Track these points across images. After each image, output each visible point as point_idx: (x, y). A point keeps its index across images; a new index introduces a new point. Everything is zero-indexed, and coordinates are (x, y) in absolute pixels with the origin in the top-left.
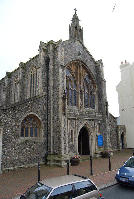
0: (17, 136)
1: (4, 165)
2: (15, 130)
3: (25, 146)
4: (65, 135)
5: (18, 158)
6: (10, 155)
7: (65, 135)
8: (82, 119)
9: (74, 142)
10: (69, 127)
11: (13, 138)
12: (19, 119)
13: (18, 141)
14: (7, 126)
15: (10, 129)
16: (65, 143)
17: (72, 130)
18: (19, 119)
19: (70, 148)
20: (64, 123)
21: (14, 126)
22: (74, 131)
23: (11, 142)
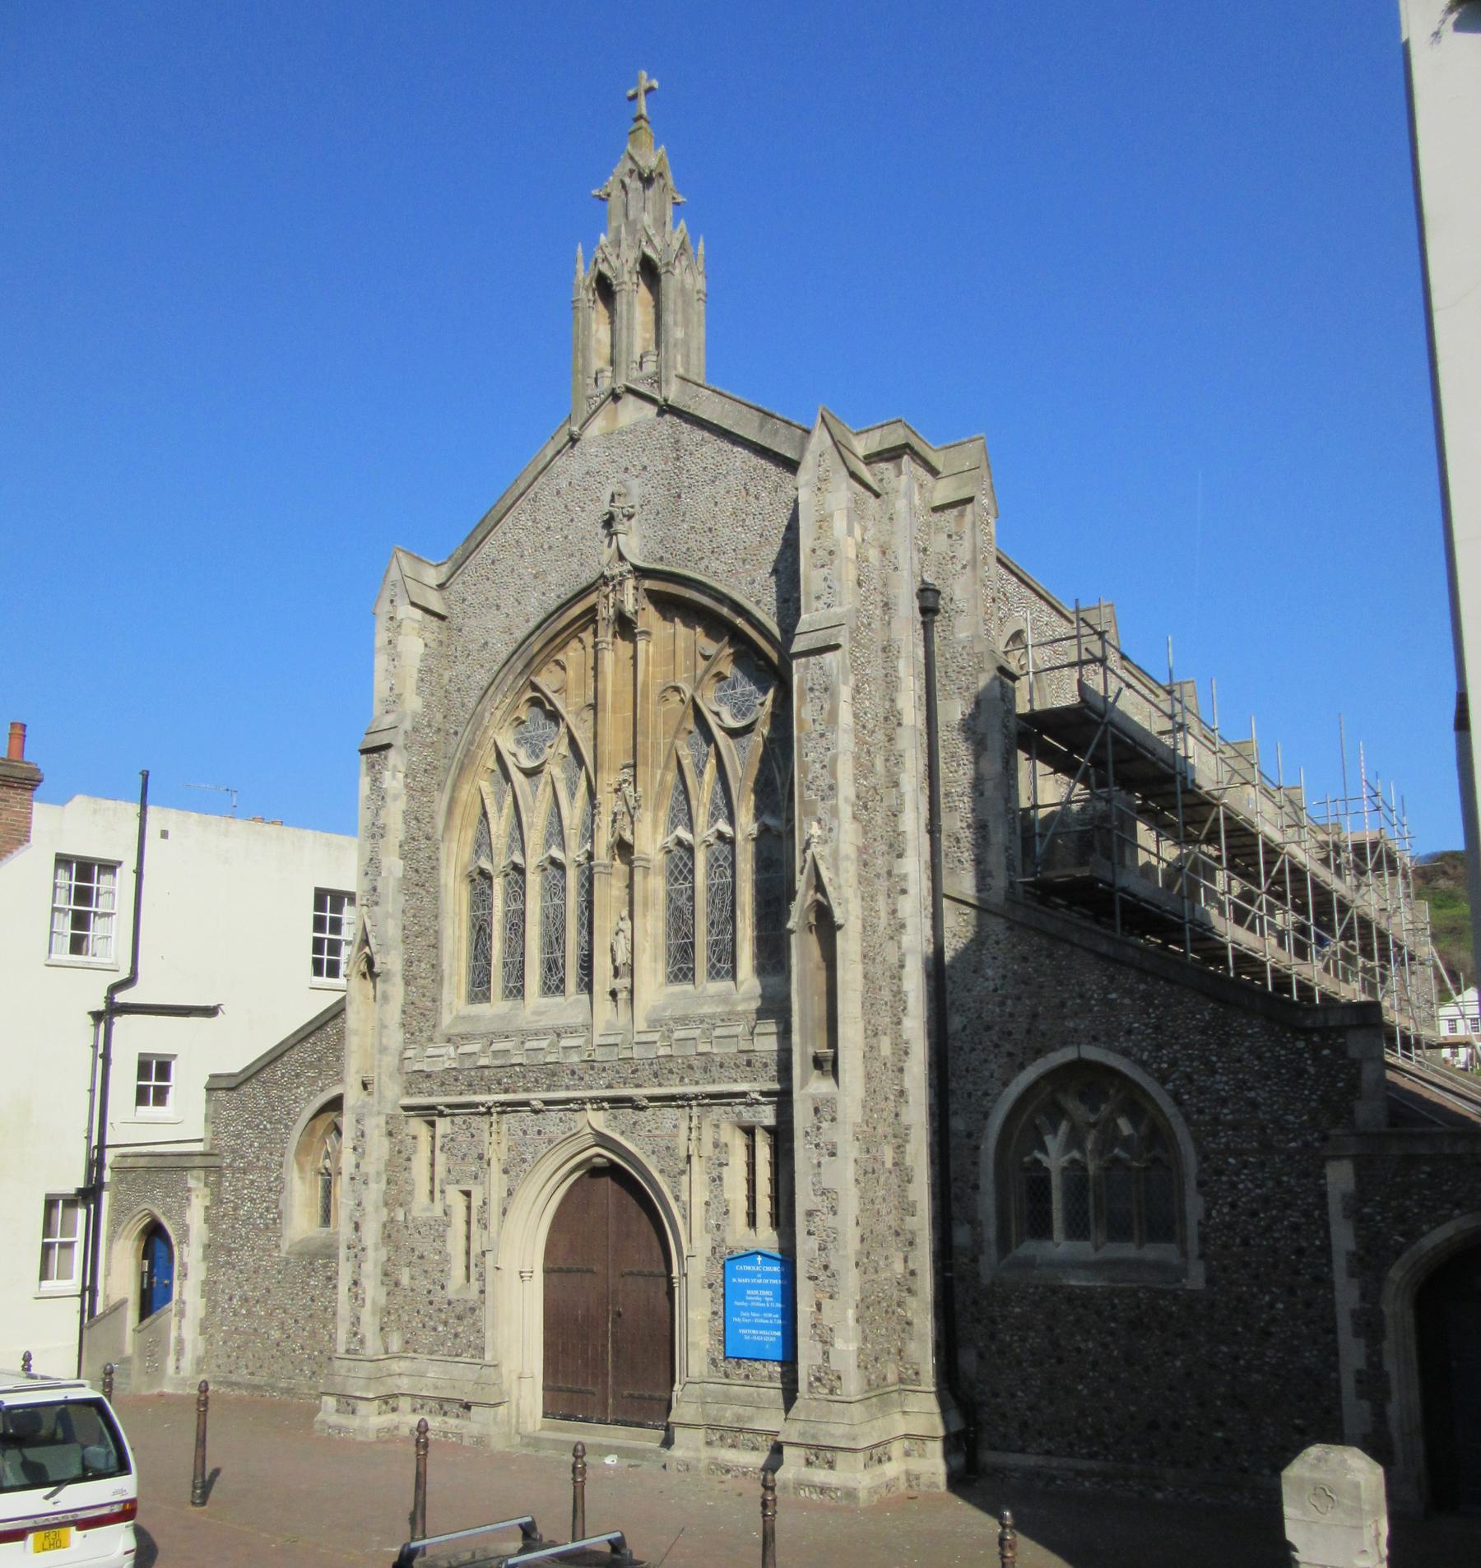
0: (274, 1220)
1: (229, 1356)
2: (270, 1190)
3: (309, 1276)
4: (357, 1227)
5: (276, 1334)
6: (249, 1312)
7: (357, 1227)
8: (547, 1103)
9: (475, 1285)
10: (440, 1169)
11: (260, 1230)
12: (286, 1126)
13: (277, 1246)
14: (239, 1168)
15: (252, 1182)
16: (355, 1283)
17: (467, 1194)
18: (286, 1126)
19: (445, 1324)
20: (355, 1149)
21: (267, 1168)
22: (476, 1202)
23: (253, 1250)
